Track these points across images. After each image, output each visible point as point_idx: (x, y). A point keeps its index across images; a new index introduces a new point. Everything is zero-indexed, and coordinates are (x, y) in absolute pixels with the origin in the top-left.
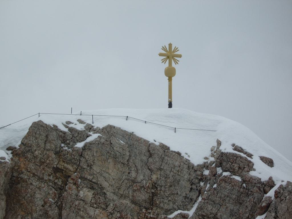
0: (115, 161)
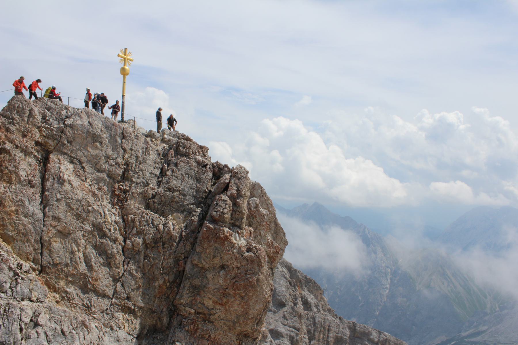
0: (94, 139)
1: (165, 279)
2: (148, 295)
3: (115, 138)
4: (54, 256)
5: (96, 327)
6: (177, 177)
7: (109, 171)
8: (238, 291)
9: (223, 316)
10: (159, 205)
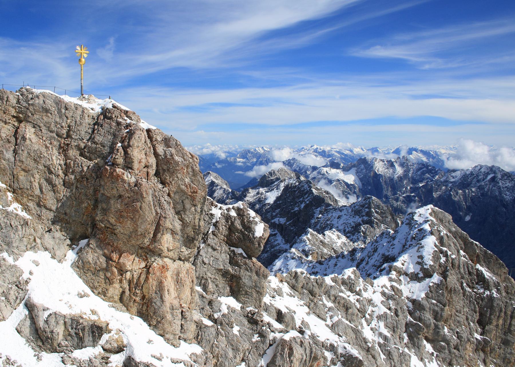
1: (88, 203)
2: (78, 213)
3: (60, 110)
4: (20, 183)
5: (42, 228)
6: (100, 134)
7: (57, 132)
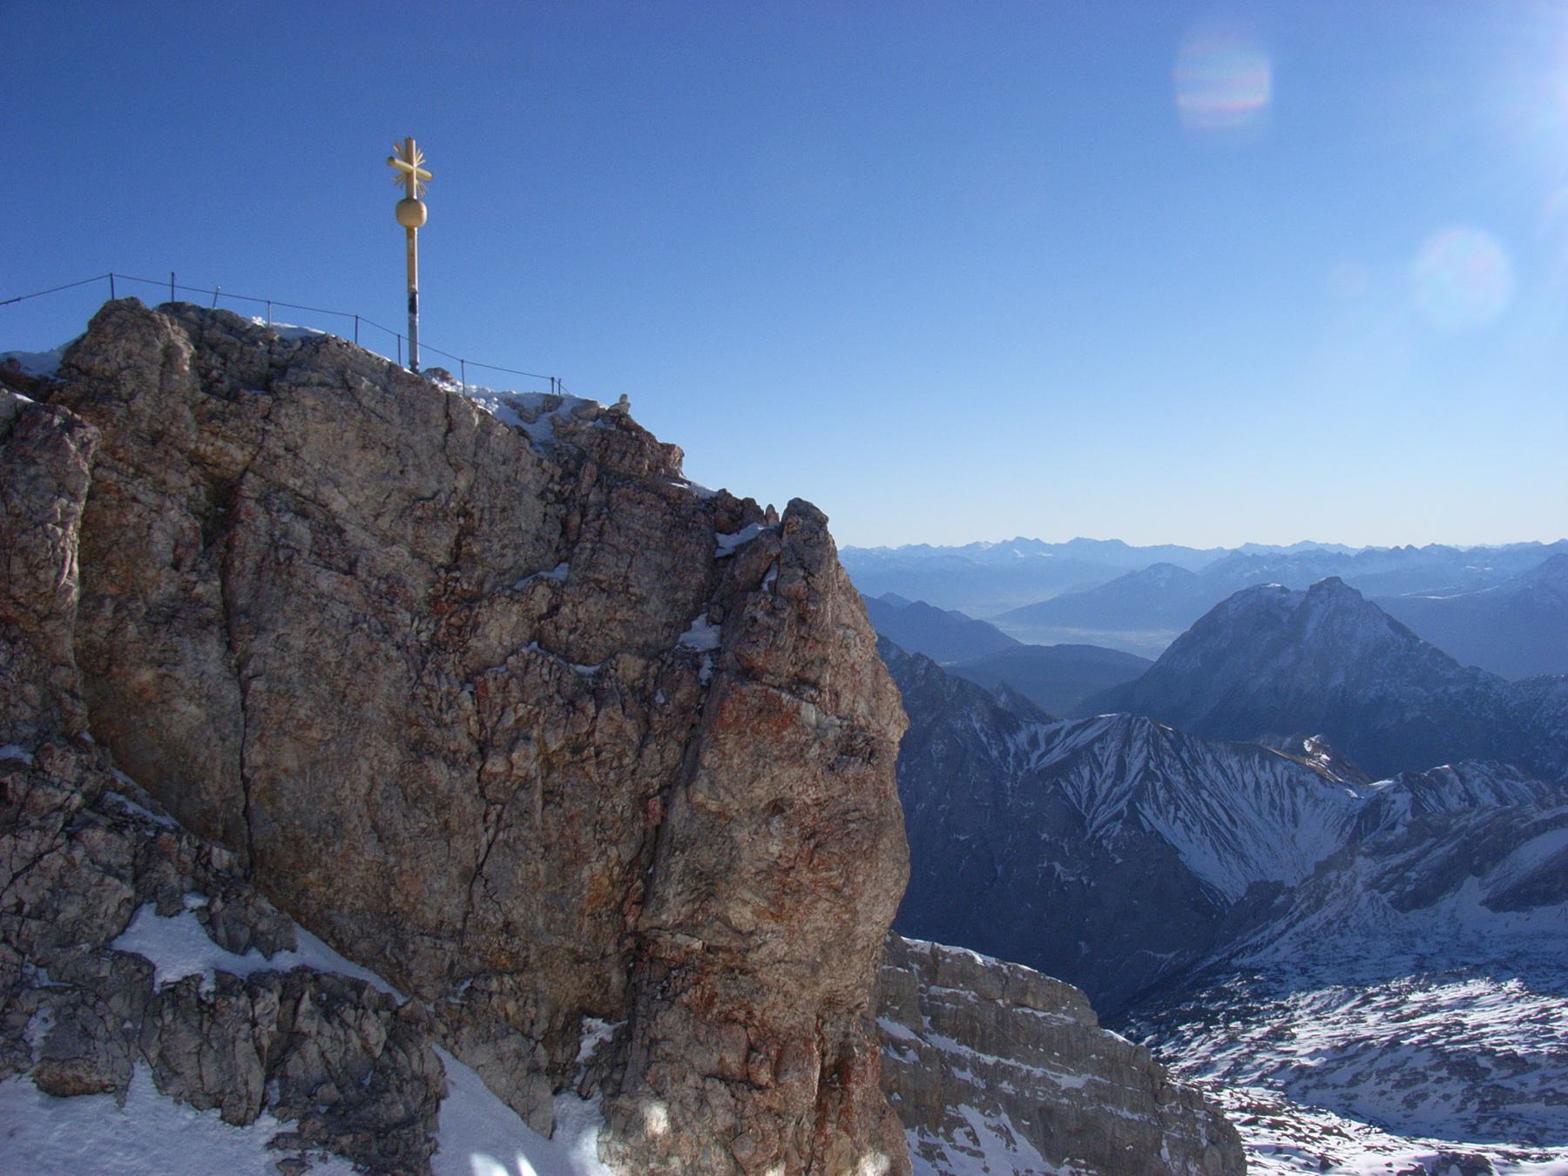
2: (562, 910)
8: (824, 874)
9: (781, 950)
10: (570, 633)
